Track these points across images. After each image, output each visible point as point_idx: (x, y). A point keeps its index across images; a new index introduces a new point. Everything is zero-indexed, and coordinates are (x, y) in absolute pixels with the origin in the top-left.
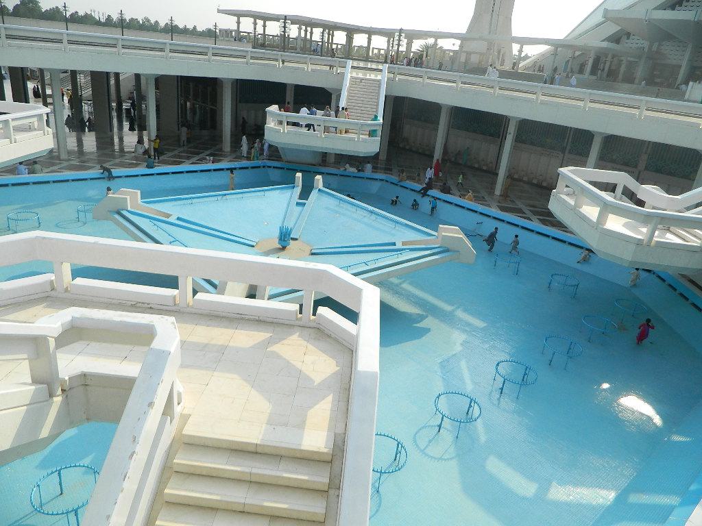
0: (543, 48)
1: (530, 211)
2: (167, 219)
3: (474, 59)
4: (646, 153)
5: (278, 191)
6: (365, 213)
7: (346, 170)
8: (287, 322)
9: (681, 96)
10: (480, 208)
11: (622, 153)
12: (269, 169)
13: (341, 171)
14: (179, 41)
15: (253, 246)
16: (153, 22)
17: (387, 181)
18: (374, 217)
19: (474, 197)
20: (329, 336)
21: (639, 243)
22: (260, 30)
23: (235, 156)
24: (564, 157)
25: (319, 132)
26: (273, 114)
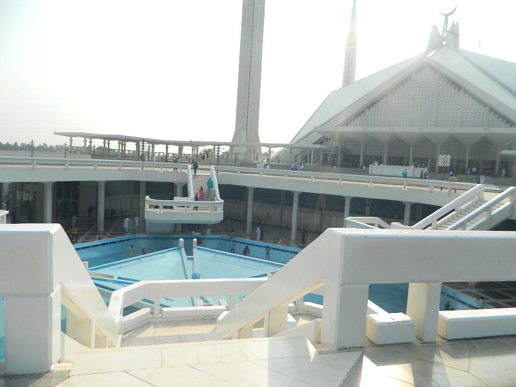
0: (279, 149)
3: (241, 157)
4: (368, 206)
5: (171, 252)
6: (236, 259)
7: (191, 235)
9: (366, 173)
12: (139, 240)
13: (188, 234)
14: (37, 157)
16: (49, 146)
18: (242, 260)
19: (283, 242)
22: (88, 144)
23: (89, 234)
25: (176, 210)
26: (148, 201)
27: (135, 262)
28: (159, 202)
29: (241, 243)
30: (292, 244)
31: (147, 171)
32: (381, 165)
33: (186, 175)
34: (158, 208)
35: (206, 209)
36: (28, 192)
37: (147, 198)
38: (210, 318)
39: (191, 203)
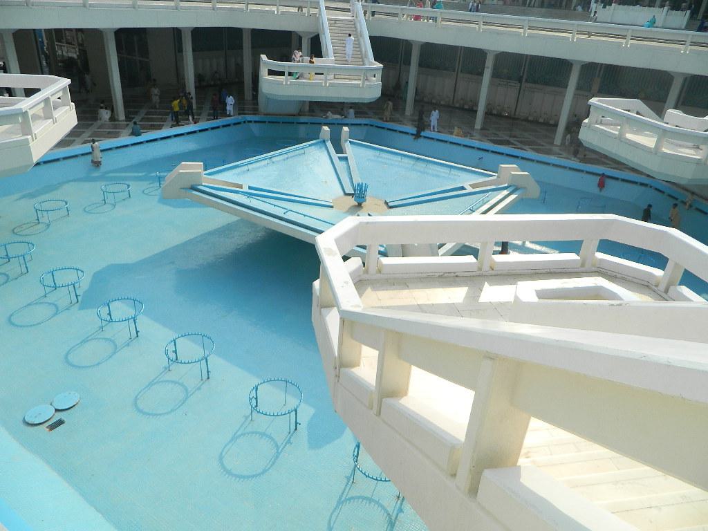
1: (518, 141)
2: (238, 189)
6: (412, 162)
8: (573, 270)
10: (476, 143)
11: (612, 80)
12: (250, 124)
15: (332, 207)
17: (371, 126)
20: (616, 277)
21: (698, 162)
24: (520, 87)
26: (265, 63)
27: (266, 162)
28: (284, 66)
29: (400, 132)
30: (478, 136)
31: (252, 11)
32: (607, 7)
33: (317, 18)
34: (284, 75)
35: (352, 77)
36: (69, 44)
37: (264, 57)
38: (453, 274)
39: (329, 69)
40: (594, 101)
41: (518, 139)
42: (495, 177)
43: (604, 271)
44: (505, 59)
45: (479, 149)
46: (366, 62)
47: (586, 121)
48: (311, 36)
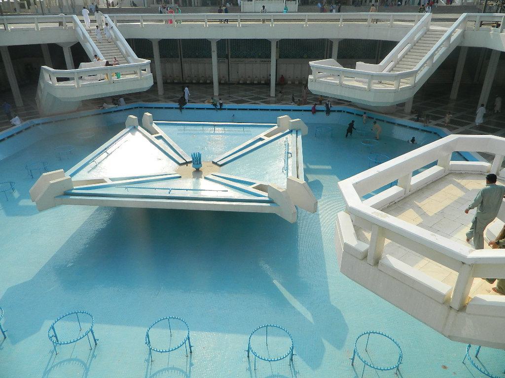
8: (441, 177)
9: (239, 11)
15: (180, 177)
17: (140, 107)
20: (461, 173)
21: (395, 91)
26: (54, 73)
33: (74, 31)
40: (311, 63)
41: (249, 97)
42: (276, 127)
43: (454, 172)
44: (222, 43)
45: (229, 109)
46: (129, 58)
47: (310, 77)
48: (70, 46)
